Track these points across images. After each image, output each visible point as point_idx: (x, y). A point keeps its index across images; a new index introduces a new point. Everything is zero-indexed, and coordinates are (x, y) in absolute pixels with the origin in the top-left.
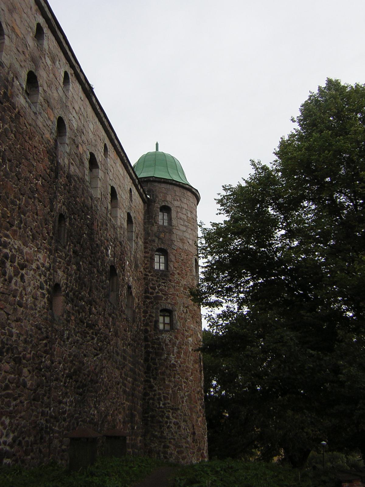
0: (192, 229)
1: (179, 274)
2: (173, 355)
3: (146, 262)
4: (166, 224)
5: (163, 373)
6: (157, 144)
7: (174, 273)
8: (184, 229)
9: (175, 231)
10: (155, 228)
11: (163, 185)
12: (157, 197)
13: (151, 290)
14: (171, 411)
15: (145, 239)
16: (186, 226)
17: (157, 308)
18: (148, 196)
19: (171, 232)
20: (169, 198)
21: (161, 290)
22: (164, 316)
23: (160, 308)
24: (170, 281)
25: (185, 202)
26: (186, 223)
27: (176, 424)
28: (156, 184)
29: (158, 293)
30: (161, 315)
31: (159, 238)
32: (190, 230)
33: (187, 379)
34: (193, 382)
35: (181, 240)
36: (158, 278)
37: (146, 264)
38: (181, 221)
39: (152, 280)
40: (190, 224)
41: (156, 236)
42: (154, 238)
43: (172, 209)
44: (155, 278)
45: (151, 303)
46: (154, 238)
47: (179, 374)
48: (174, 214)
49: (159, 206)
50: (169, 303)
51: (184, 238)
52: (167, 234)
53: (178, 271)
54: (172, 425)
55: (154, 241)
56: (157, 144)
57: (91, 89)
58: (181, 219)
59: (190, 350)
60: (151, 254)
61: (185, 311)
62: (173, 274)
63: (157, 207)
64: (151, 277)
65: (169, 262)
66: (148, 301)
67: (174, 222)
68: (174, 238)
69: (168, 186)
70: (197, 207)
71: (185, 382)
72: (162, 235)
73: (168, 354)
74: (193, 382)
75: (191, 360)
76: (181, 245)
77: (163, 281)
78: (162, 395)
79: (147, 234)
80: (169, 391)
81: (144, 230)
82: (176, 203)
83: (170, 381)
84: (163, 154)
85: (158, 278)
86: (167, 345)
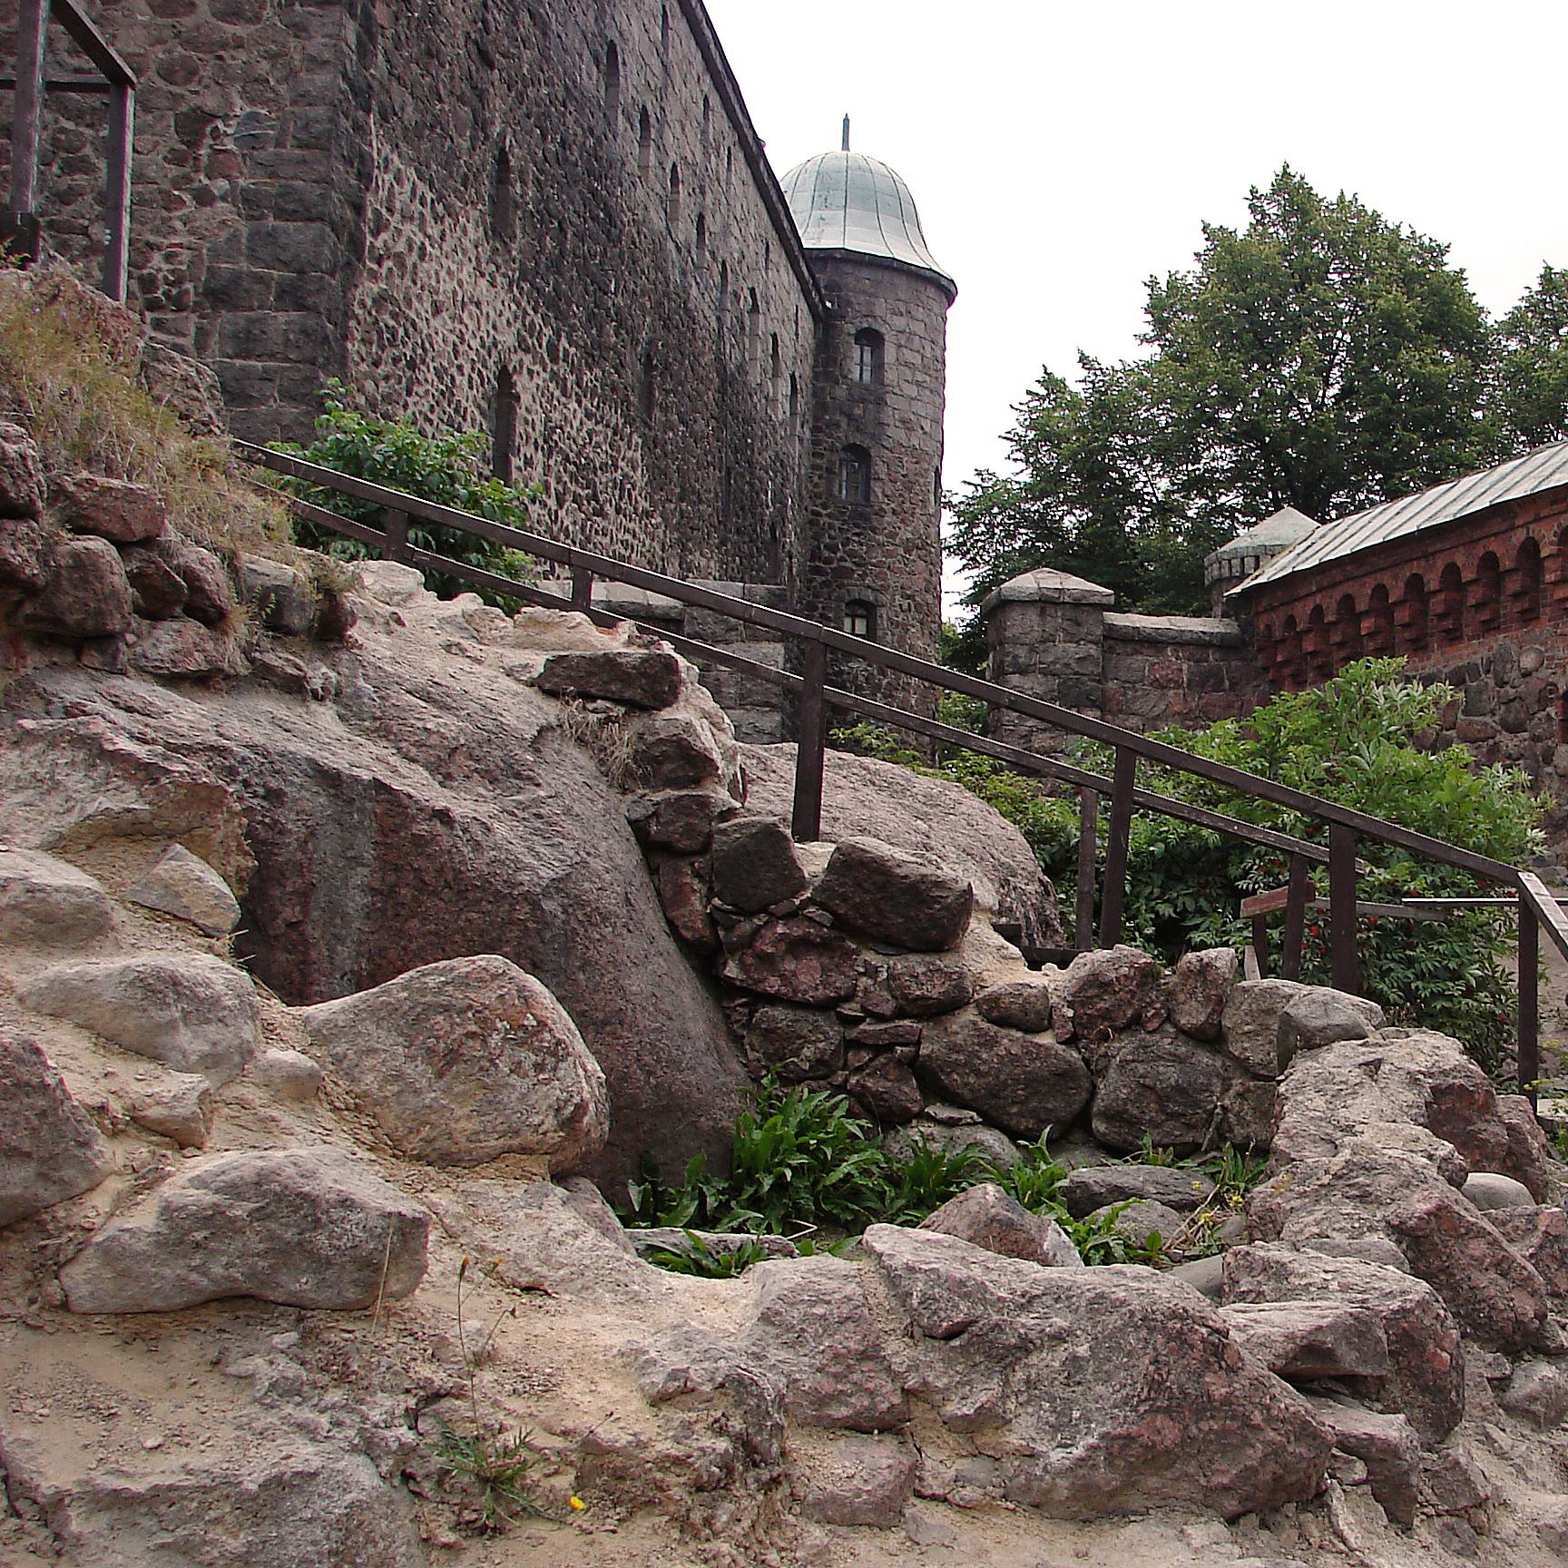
0: (931, 391)
1: (894, 512)
3: (816, 479)
4: (867, 376)
6: (846, 121)
8: (912, 391)
9: (890, 399)
10: (841, 391)
11: (865, 273)
12: (849, 304)
13: (826, 553)
15: (816, 418)
16: (918, 384)
17: (839, 599)
18: (829, 304)
19: (880, 402)
20: (881, 308)
21: (852, 554)
22: (854, 617)
23: (847, 598)
24: (874, 530)
25: (921, 317)
26: (920, 377)
28: (848, 268)
29: (842, 559)
30: (847, 615)
31: (850, 417)
32: (928, 393)
35: (903, 422)
36: (845, 522)
37: (816, 486)
38: (907, 371)
39: (831, 527)
40: (928, 378)
41: (842, 413)
42: (837, 417)
43: (886, 337)
44: (837, 524)
45: (825, 584)
46: (837, 417)
48: (890, 354)
49: (853, 331)
50: (869, 587)
51: (912, 417)
52: (871, 406)
53: (893, 505)
55: (838, 426)
56: (846, 121)
57: (760, 144)
58: (906, 364)
60: (829, 461)
61: (905, 607)
62: (881, 513)
63: (849, 334)
64: (826, 519)
65: (872, 482)
66: (819, 579)
67: (890, 376)
68: (888, 416)
69: (878, 275)
70: (950, 313)
72: (858, 411)
76: (904, 437)
77: (857, 531)
79: (820, 405)
81: (814, 395)
82: (900, 322)
84: (865, 169)
85: (845, 522)
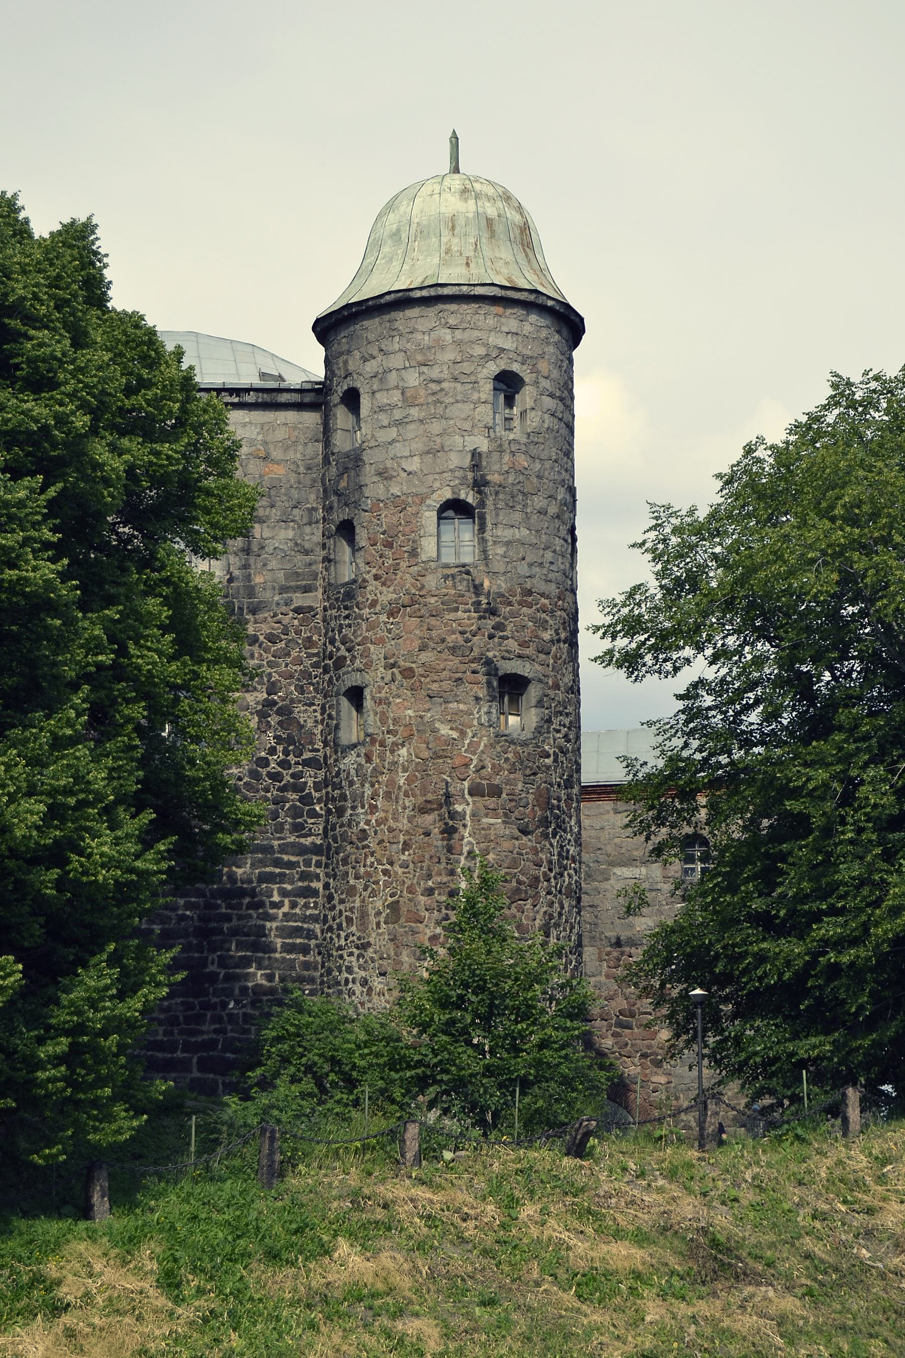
1: (376, 577)
2: (363, 807)
5: (345, 861)
6: (455, 140)
7: (364, 581)
14: (356, 952)
27: (365, 982)
33: (391, 864)
34: (411, 865)
47: (372, 854)
54: (357, 988)
56: (455, 140)
59: (402, 782)
61: (388, 678)
71: (386, 872)
73: (354, 808)
74: (411, 865)
75: (405, 808)
78: (345, 914)
80: (354, 902)
83: (357, 877)
86: (352, 783)
